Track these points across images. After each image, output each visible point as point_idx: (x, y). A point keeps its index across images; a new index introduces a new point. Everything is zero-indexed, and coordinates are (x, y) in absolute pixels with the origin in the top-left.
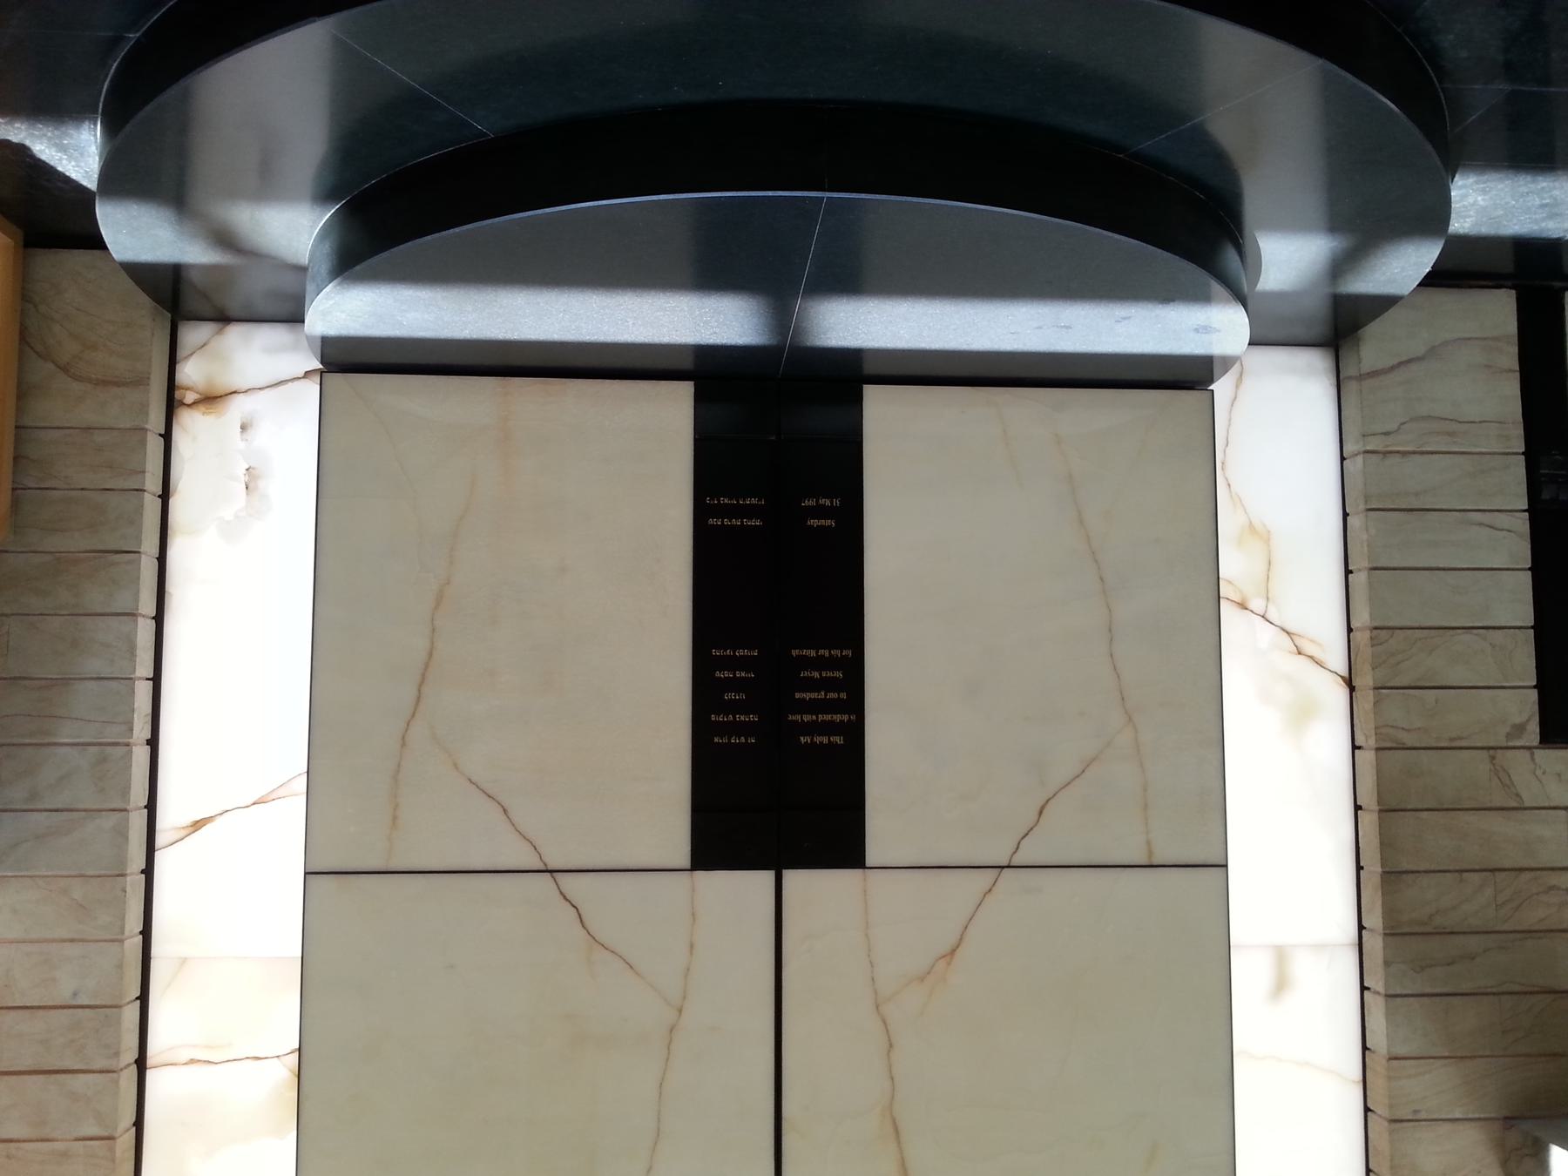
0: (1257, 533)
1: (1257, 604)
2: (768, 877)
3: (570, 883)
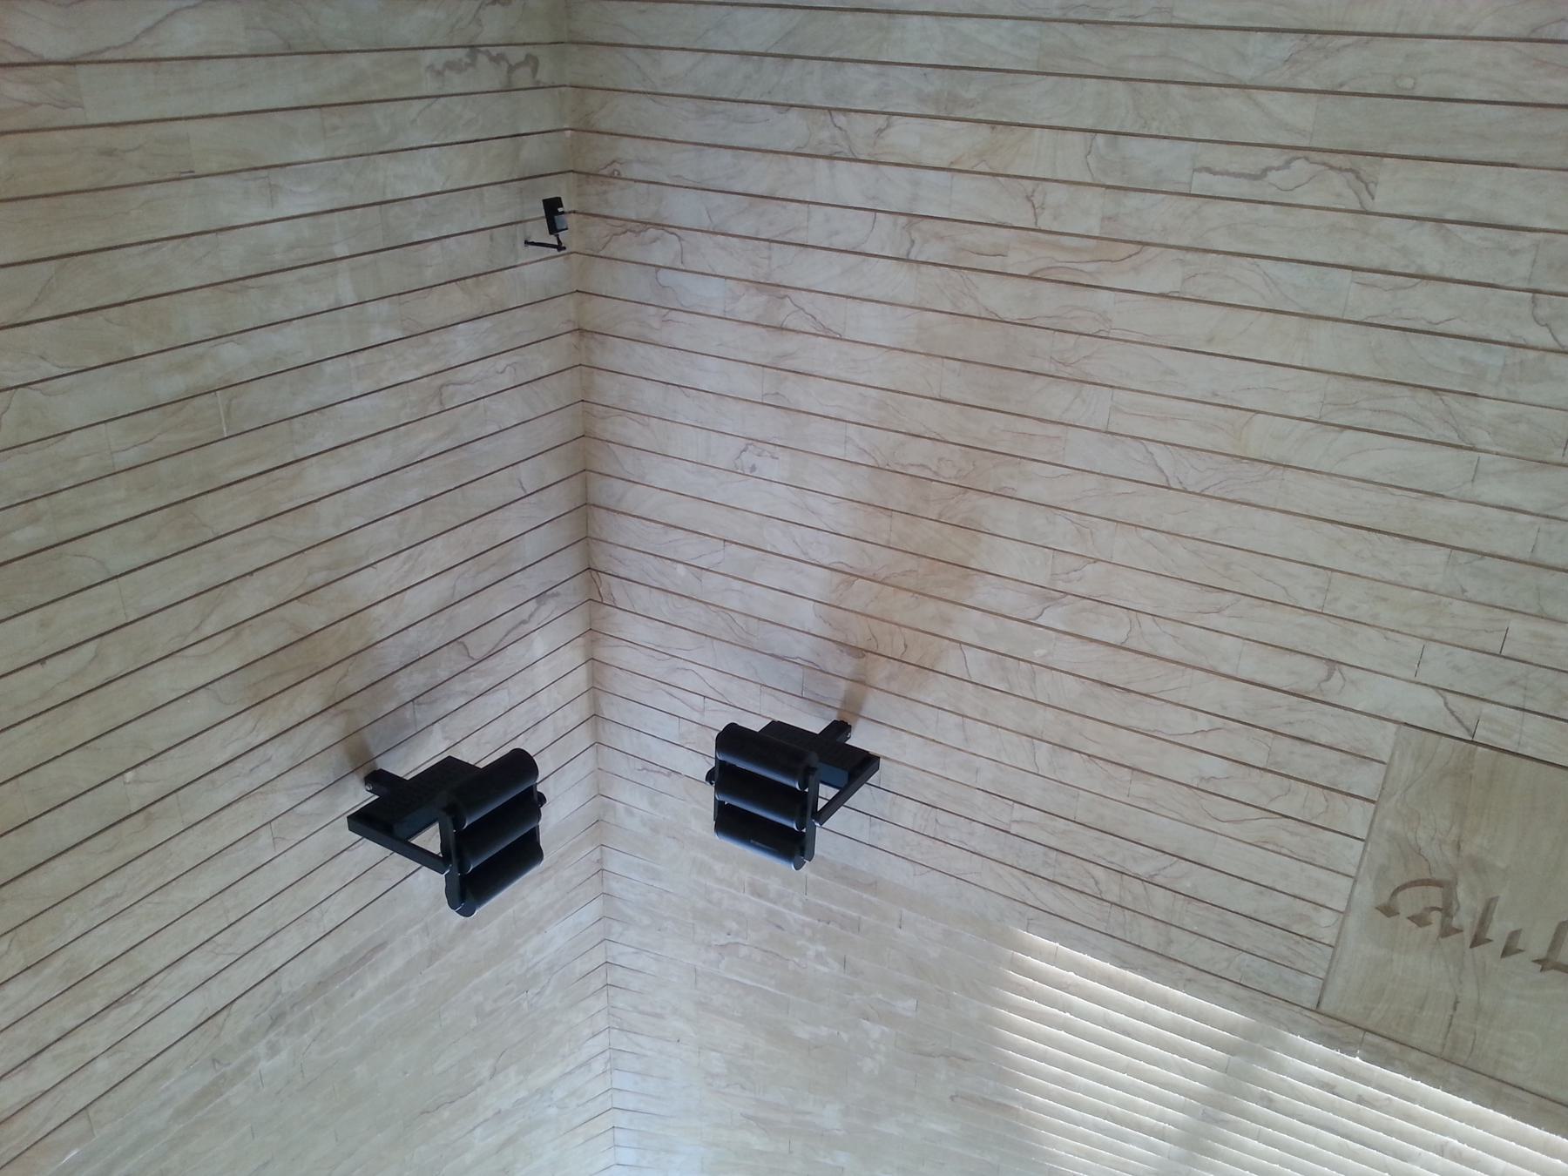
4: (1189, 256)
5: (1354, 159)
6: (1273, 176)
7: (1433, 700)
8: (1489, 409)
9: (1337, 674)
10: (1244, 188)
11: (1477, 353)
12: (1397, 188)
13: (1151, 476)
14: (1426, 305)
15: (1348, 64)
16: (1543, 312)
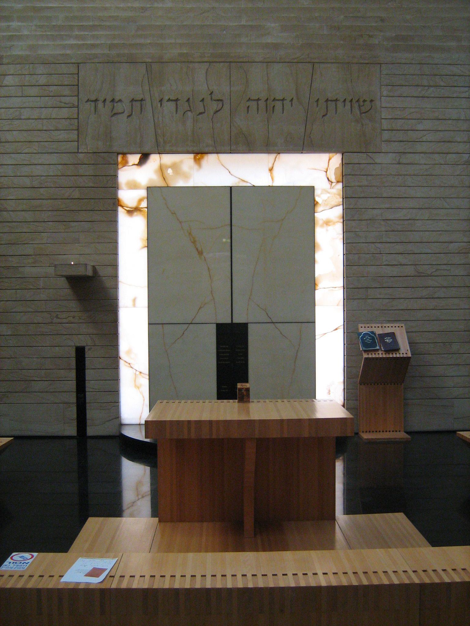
0: (138, 387)
1: (138, 373)
2: (234, 322)
3: (269, 321)
4: (448, 252)
5: (420, 275)
6: (434, 270)
7: (377, 161)
8: (383, 229)
9: (397, 161)
10: (439, 267)
11: (388, 240)
12: (410, 270)
13: (448, 200)
14: (399, 248)
15: (425, 293)
16: (379, 250)
